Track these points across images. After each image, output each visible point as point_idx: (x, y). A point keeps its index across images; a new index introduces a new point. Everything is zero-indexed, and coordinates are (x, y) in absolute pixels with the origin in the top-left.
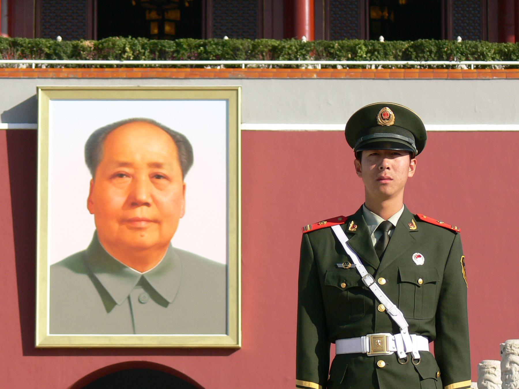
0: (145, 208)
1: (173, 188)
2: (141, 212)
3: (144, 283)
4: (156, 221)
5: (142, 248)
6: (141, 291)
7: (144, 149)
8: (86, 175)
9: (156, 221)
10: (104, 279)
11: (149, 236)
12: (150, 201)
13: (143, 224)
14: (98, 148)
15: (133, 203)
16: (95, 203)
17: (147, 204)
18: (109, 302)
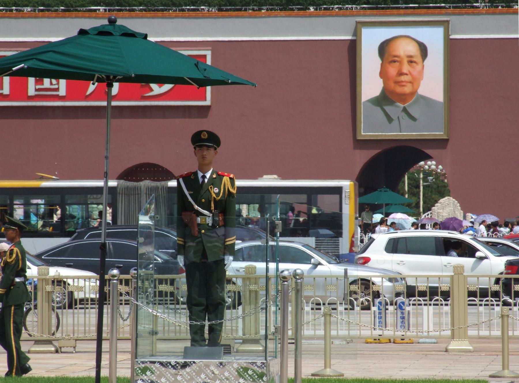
0: (405, 76)
1: (418, 67)
3: (405, 110)
4: (410, 82)
5: (404, 95)
6: (403, 114)
8: (379, 61)
9: (410, 82)
10: (388, 108)
11: (407, 89)
12: (408, 73)
13: (404, 84)
14: (384, 49)
15: (400, 74)
16: (383, 74)
17: (407, 74)
18: (390, 119)
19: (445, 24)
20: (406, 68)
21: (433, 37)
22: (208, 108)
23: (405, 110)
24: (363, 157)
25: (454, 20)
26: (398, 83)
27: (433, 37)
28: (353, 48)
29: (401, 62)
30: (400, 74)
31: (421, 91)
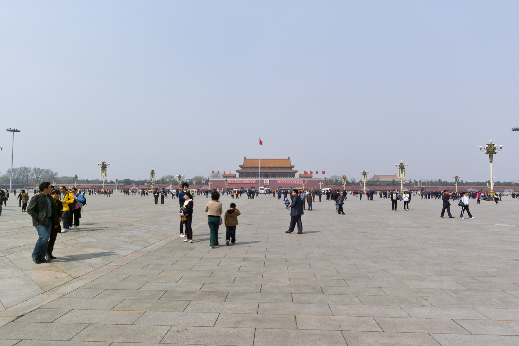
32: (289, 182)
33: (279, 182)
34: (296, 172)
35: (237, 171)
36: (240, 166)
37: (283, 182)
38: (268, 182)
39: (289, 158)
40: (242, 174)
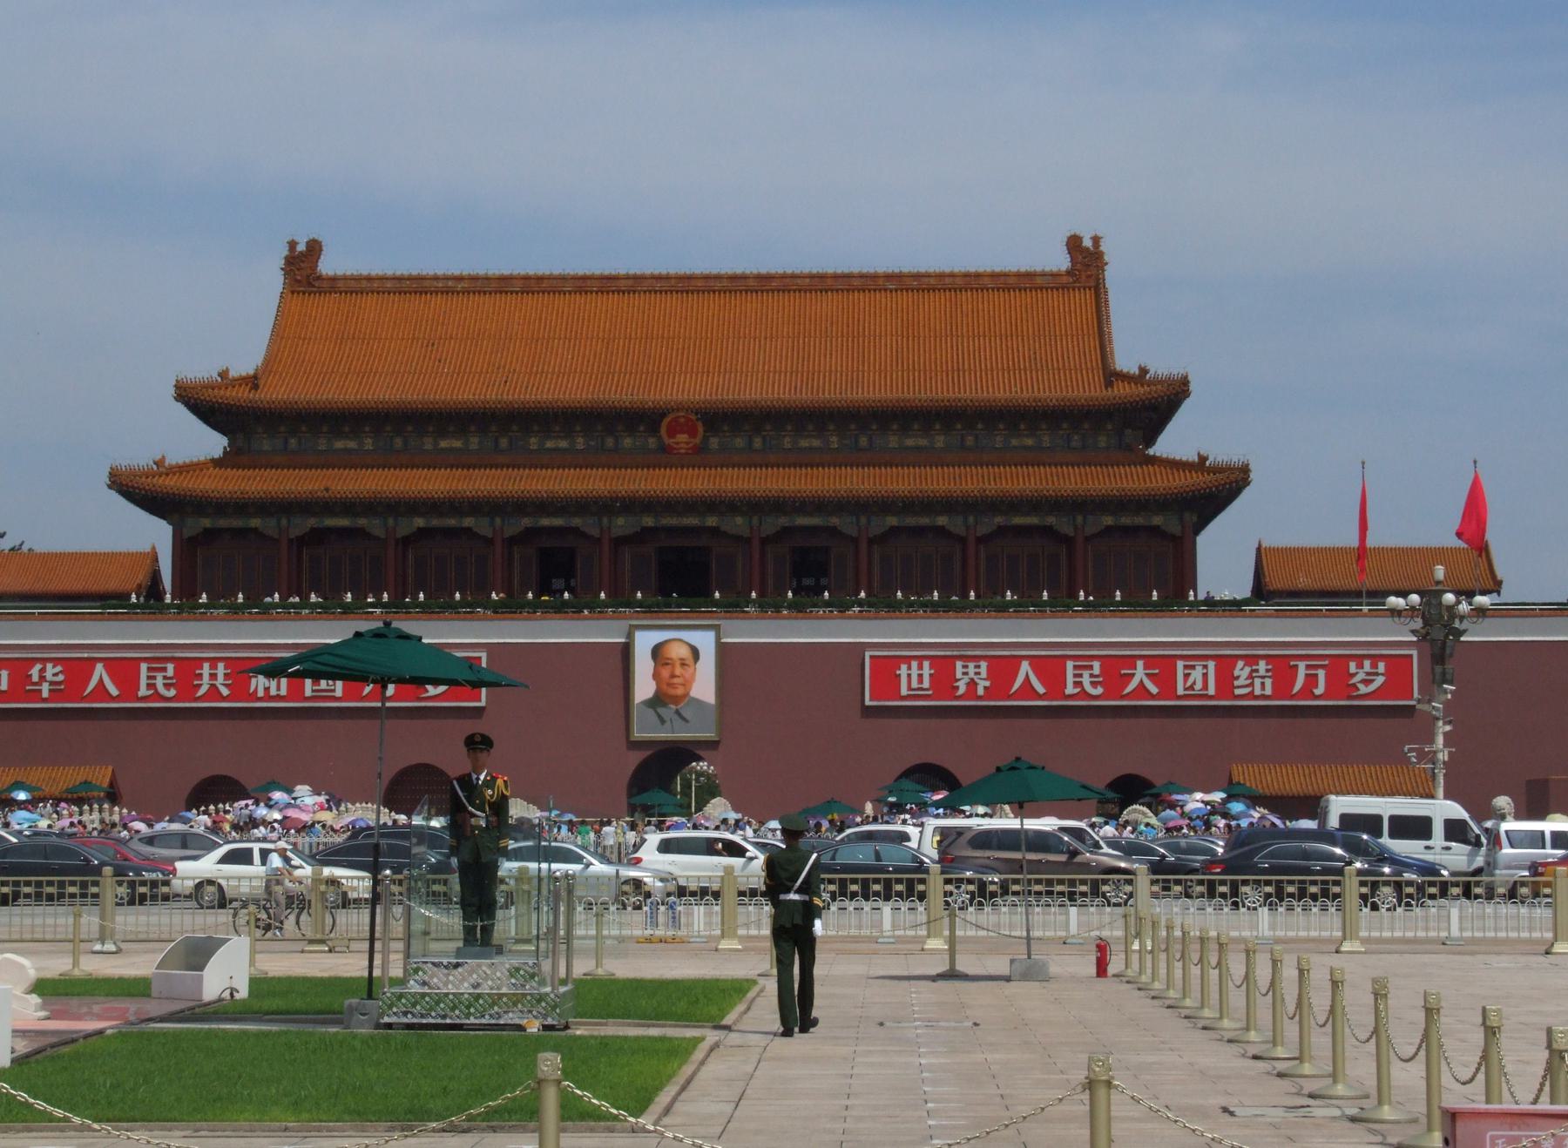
2: (676, 680)
3: (677, 712)
7: (678, 652)
11: (680, 691)
14: (657, 652)
15: (673, 676)
16: (656, 676)
18: (663, 721)
19: (716, 628)
20: (678, 671)
21: (705, 641)
22: (483, 709)
23: (677, 712)
24: (636, 758)
25: (725, 624)
26: (669, 685)
27: (705, 641)
28: (626, 652)
29: (673, 666)
30: (673, 676)
31: (693, 693)
32: (1081, 683)
33: (914, 679)
34: (1217, 489)
35: (137, 489)
36: (202, 403)
37: (972, 677)
38: (704, 686)
39: (1087, 261)
40: (222, 544)
